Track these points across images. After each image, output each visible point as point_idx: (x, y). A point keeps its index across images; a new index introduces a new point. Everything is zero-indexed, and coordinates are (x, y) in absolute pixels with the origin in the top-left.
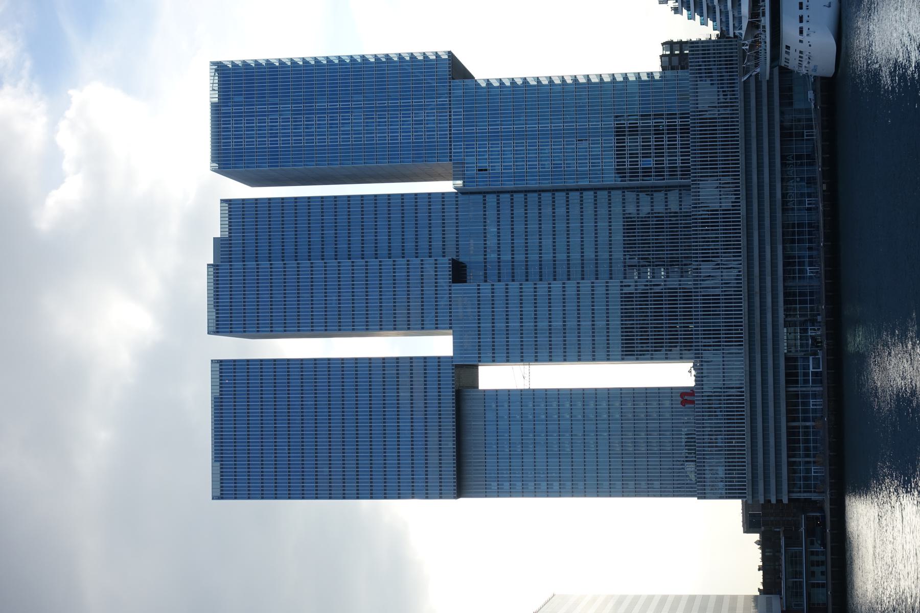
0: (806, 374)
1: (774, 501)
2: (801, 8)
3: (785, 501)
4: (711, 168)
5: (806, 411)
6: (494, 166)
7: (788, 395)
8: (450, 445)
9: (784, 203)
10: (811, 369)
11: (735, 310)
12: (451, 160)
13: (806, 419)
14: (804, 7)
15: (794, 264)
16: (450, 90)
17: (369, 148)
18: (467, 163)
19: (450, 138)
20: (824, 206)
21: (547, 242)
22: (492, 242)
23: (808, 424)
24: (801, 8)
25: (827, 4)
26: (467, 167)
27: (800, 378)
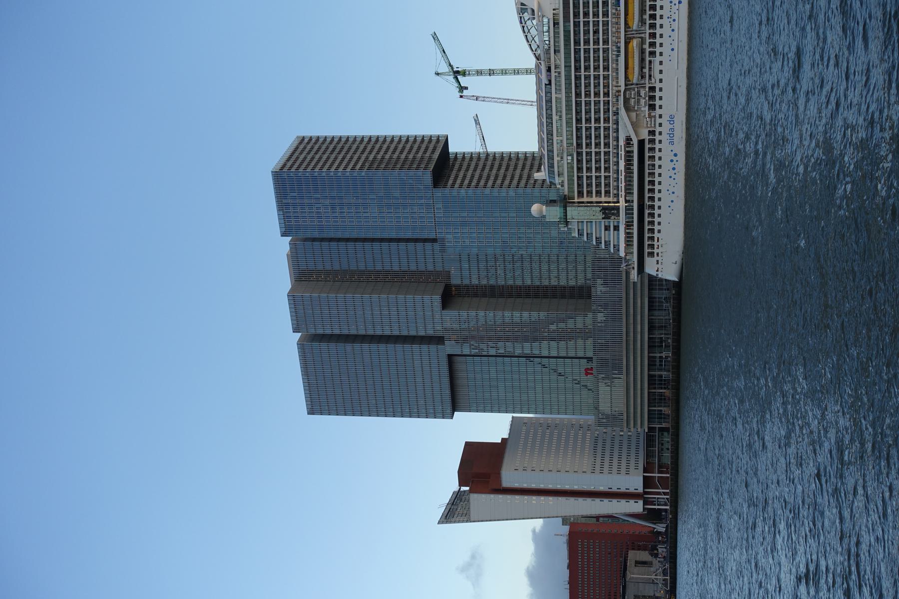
2: (658, 263)
4: (602, 267)
6: (465, 241)
7: (649, 376)
8: (447, 392)
11: (618, 315)
13: (661, 370)
14: (660, 263)
16: (433, 195)
17: (382, 228)
18: (447, 239)
19: (436, 228)
24: (658, 263)
25: (674, 262)
27: (658, 363)
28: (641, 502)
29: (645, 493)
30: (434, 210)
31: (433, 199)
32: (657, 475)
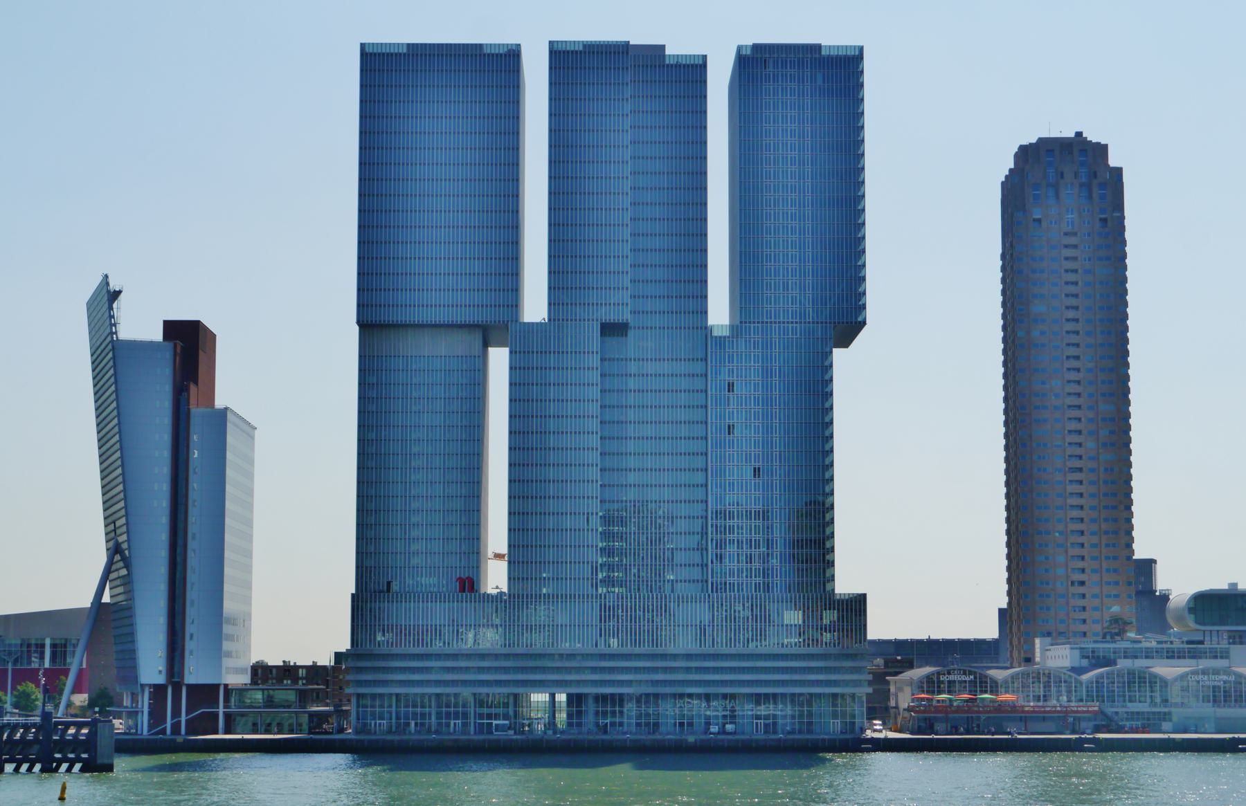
0: (489, 716)
5: (448, 715)
9: (682, 696)
12: (741, 322)
15: (613, 705)
16: (822, 323)
17: (758, 228)
18: (737, 341)
20: (671, 740)
21: (649, 431)
22: (650, 368)
23: (433, 717)
26: (733, 341)
28: (161, 679)
29: (177, 687)
30: (792, 323)
31: (813, 323)
32: (221, 710)
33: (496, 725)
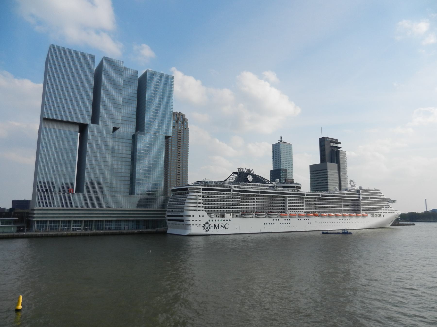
0: (76, 226)
1: (34, 216)
3: (34, 220)
10: (77, 228)
23: (60, 227)
27: (75, 225)
33: (78, 228)
